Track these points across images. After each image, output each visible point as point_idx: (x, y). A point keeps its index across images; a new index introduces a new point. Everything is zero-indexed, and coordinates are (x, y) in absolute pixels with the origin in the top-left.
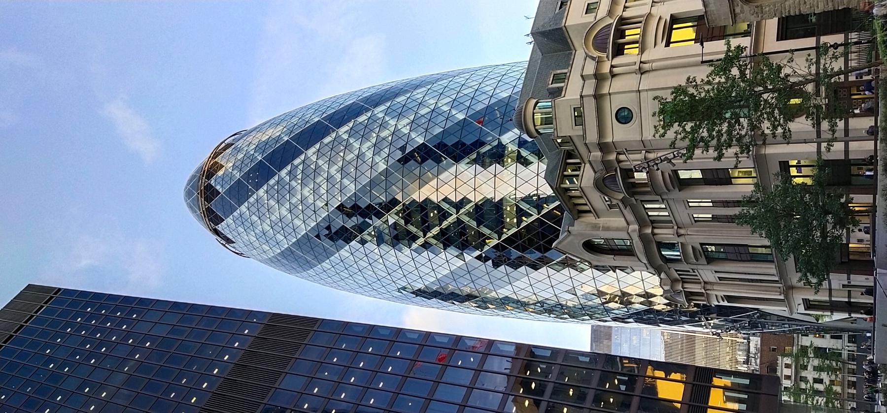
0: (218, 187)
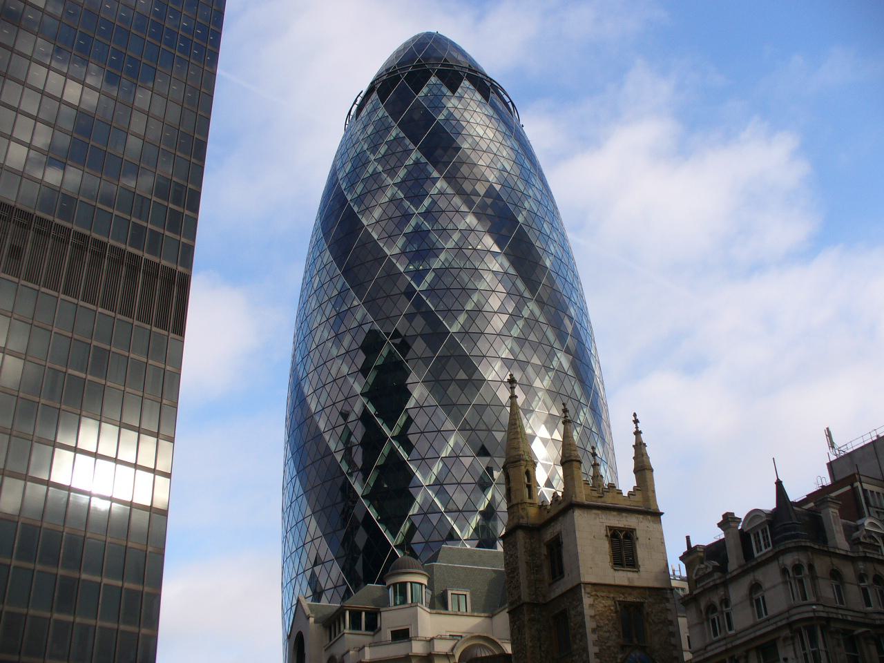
0: (425, 90)
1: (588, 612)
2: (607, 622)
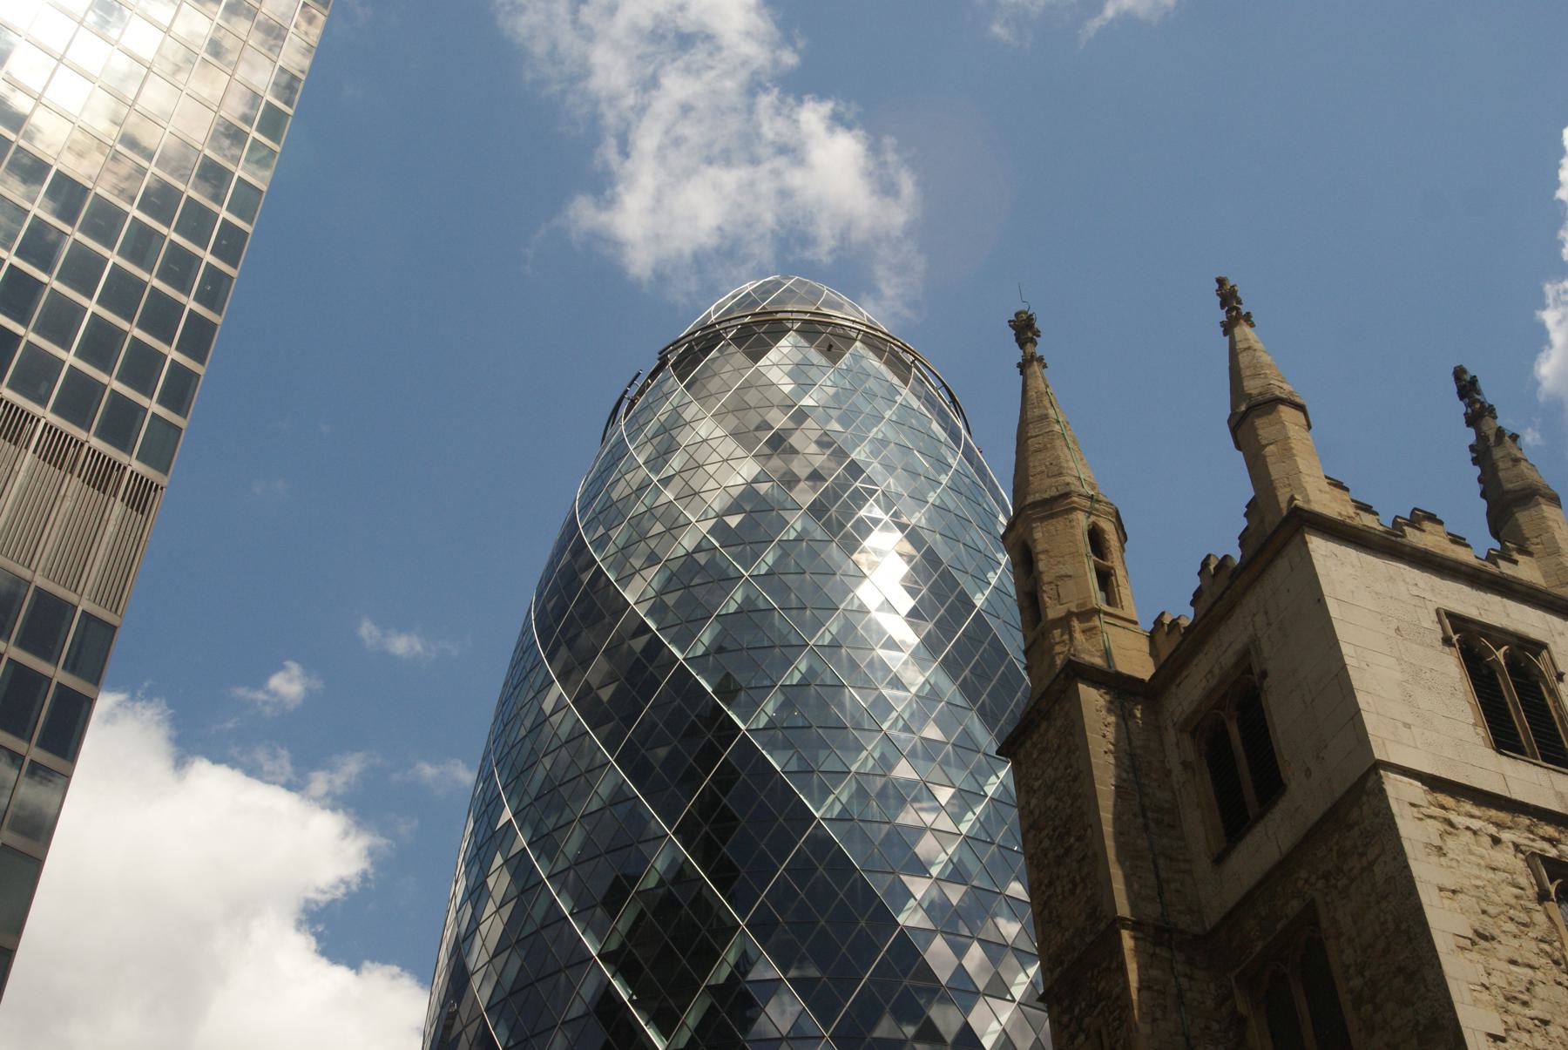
1: (1426, 873)
2: (1510, 927)
